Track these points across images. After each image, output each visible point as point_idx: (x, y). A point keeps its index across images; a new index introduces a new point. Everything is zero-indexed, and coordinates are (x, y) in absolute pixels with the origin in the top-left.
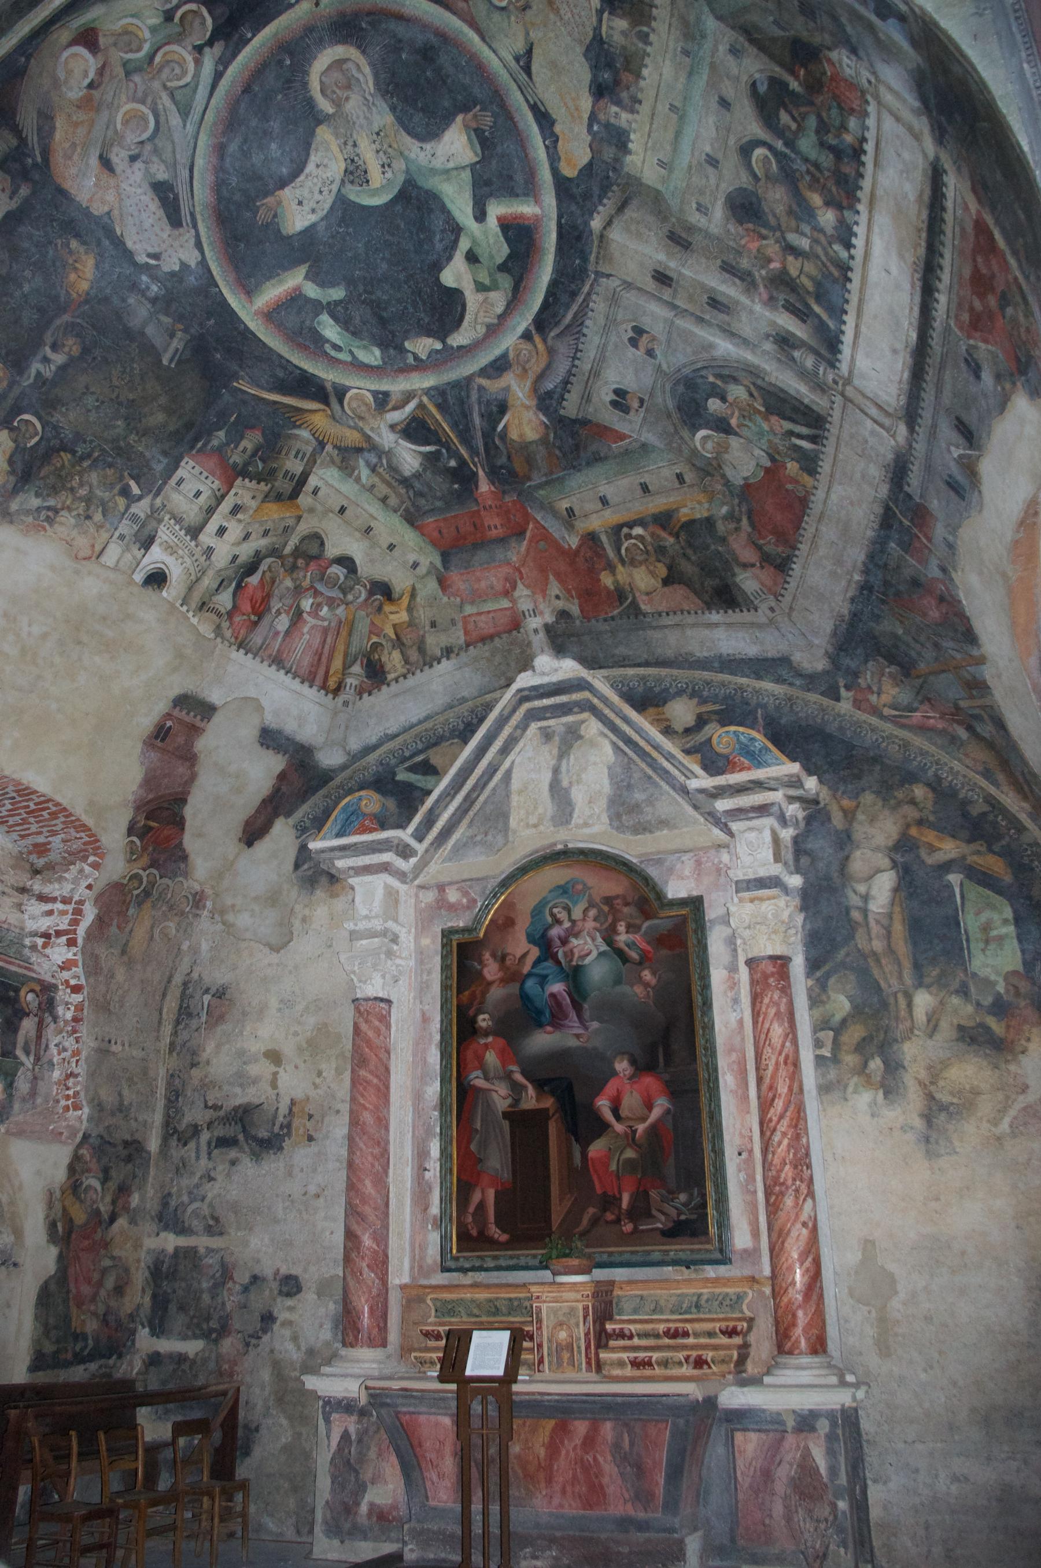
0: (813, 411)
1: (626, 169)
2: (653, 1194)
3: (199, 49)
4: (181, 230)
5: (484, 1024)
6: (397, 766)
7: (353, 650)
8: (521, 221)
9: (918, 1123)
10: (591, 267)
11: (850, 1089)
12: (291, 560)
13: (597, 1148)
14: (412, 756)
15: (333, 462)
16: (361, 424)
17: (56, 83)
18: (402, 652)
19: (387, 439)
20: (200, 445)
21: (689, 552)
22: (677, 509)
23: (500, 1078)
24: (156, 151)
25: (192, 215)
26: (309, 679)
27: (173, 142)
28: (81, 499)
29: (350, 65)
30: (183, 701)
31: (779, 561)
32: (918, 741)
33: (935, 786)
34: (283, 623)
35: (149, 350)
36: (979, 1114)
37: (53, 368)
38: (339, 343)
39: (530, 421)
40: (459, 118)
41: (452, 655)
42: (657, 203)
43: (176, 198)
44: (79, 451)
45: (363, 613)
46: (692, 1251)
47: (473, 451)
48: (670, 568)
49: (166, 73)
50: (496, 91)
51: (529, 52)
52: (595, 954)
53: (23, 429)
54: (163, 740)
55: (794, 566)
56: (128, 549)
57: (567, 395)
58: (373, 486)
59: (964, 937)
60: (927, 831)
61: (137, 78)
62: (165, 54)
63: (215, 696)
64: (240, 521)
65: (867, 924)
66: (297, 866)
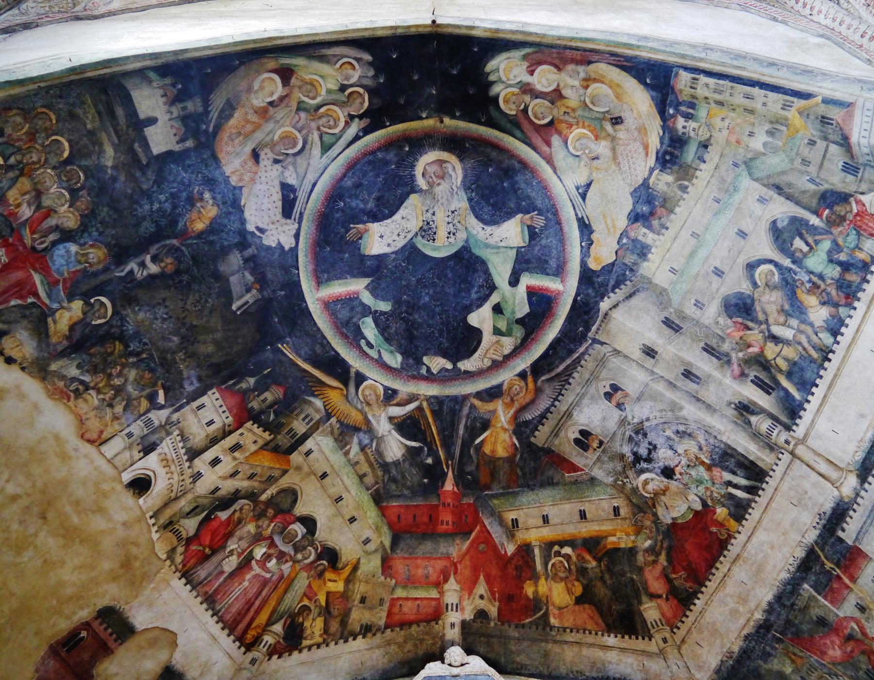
0: (757, 466)
1: (641, 271)
3: (352, 117)
4: (288, 221)
7: (282, 608)
8: (545, 293)
10: (590, 335)
12: (262, 507)
15: (332, 433)
16: (366, 409)
17: (249, 90)
19: (383, 427)
20: (231, 382)
21: (607, 576)
22: (606, 537)
24: (294, 164)
25: (301, 214)
26: (230, 626)
27: (309, 164)
28: (113, 387)
29: (448, 165)
31: (685, 595)
34: (231, 564)
35: (227, 296)
37: (145, 273)
38: (373, 342)
39: (504, 441)
40: (519, 216)
41: (369, 635)
42: (662, 297)
43: (295, 199)
44: (132, 347)
45: (304, 574)
47: (450, 455)
48: (587, 588)
49: (324, 120)
50: (554, 205)
51: (589, 185)
53: (97, 307)
55: (696, 601)
56: (130, 447)
57: (540, 428)
58: (357, 463)
61: (303, 115)
62: (329, 110)
63: (140, 619)
64: (235, 459)
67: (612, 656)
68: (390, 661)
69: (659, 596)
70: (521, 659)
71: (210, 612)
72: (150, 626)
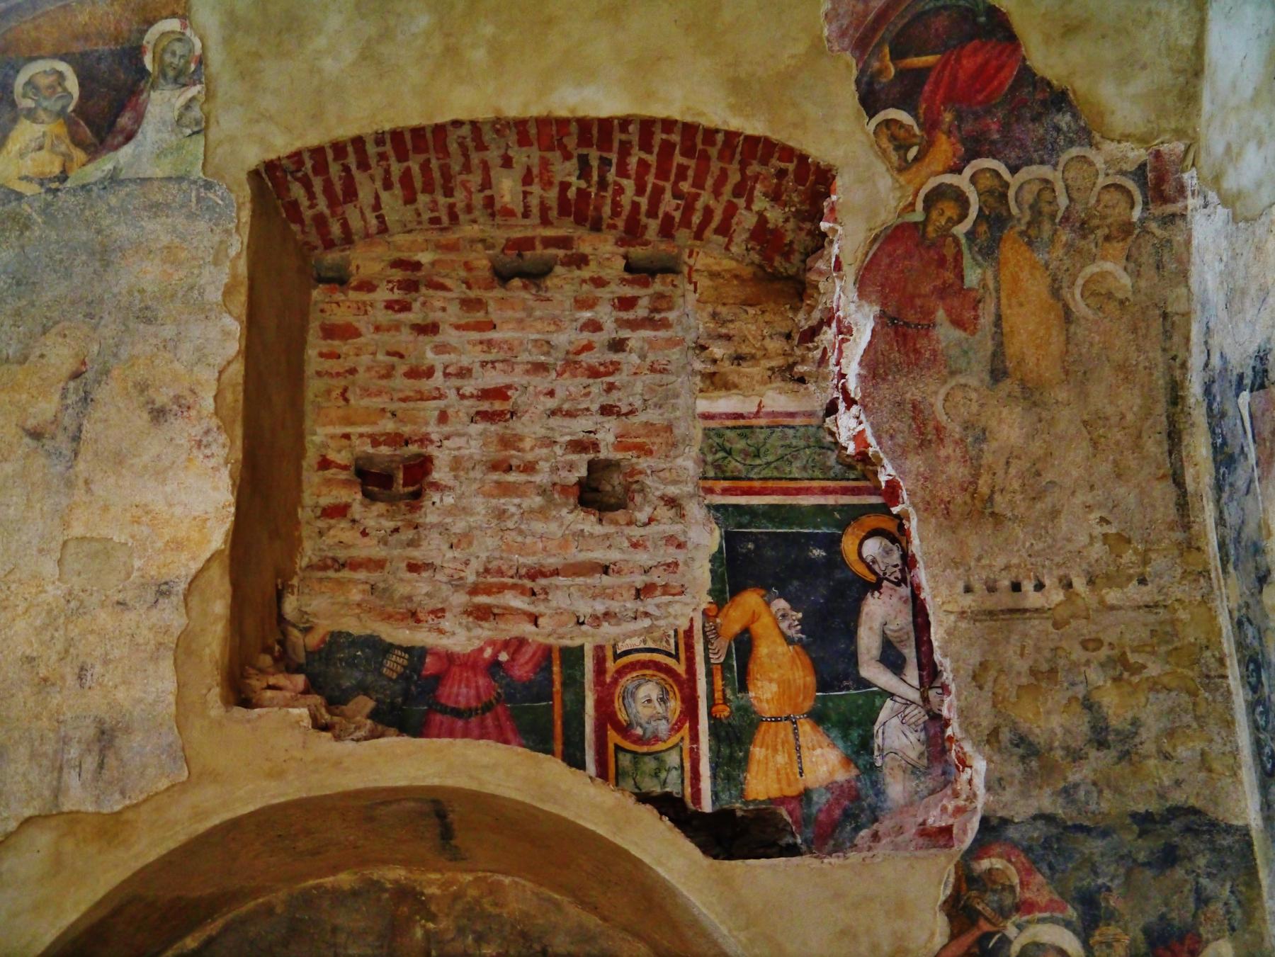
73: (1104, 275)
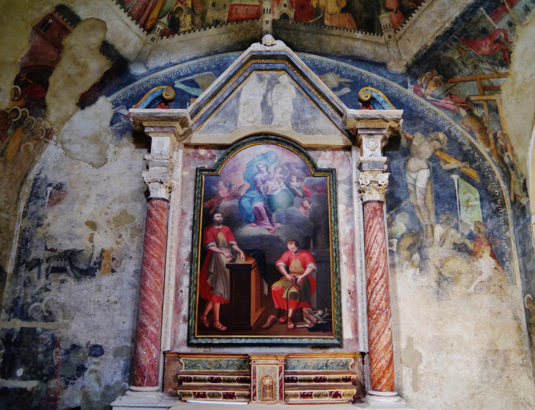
2: (305, 310)
5: (218, 219)
6: (175, 79)
7: (166, 8)
9: (434, 284)
11: (404, 267)
13: (277, 285)
14: (184, 76)
18: (192, 17)
23: (226, 247)
26: (136, 18)
30: (62, 9)
32: (442, 113)
33: (448, 134)
36: (461, 283)
41: (218, 26)
46: (324, 338)
52: (280, 190)
54: (45, 31)
59: (458, 204)
60: (443, 154)
63: (82, 13)
65: (415, 192)
66: (112, 123)
67: (358, 44)
68: (231, 42)
69: (392, 10)
70: (305, 43)
71: (123, 10)
72: (89, 17)
73: (30, 145)
